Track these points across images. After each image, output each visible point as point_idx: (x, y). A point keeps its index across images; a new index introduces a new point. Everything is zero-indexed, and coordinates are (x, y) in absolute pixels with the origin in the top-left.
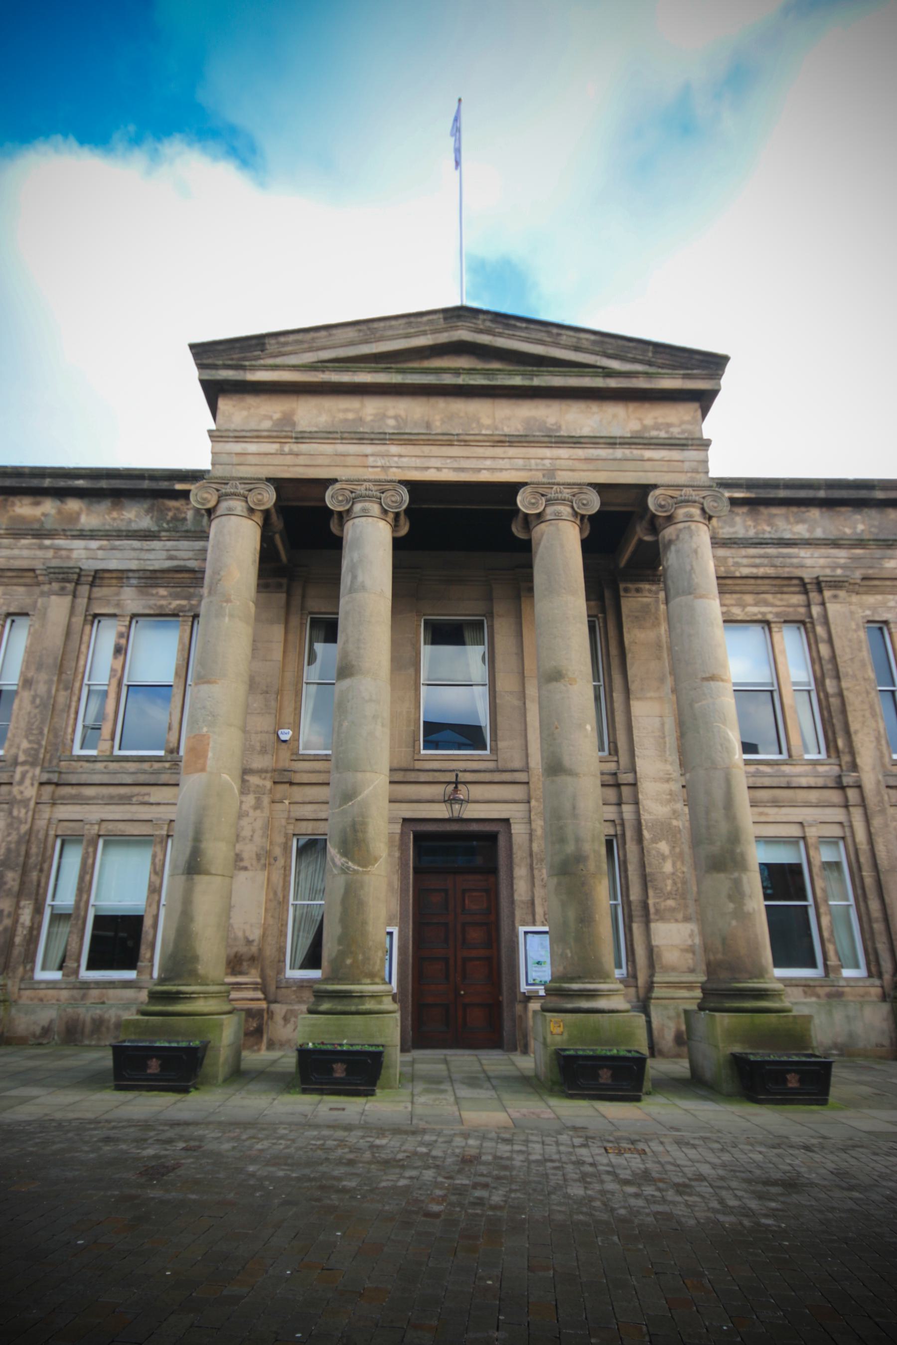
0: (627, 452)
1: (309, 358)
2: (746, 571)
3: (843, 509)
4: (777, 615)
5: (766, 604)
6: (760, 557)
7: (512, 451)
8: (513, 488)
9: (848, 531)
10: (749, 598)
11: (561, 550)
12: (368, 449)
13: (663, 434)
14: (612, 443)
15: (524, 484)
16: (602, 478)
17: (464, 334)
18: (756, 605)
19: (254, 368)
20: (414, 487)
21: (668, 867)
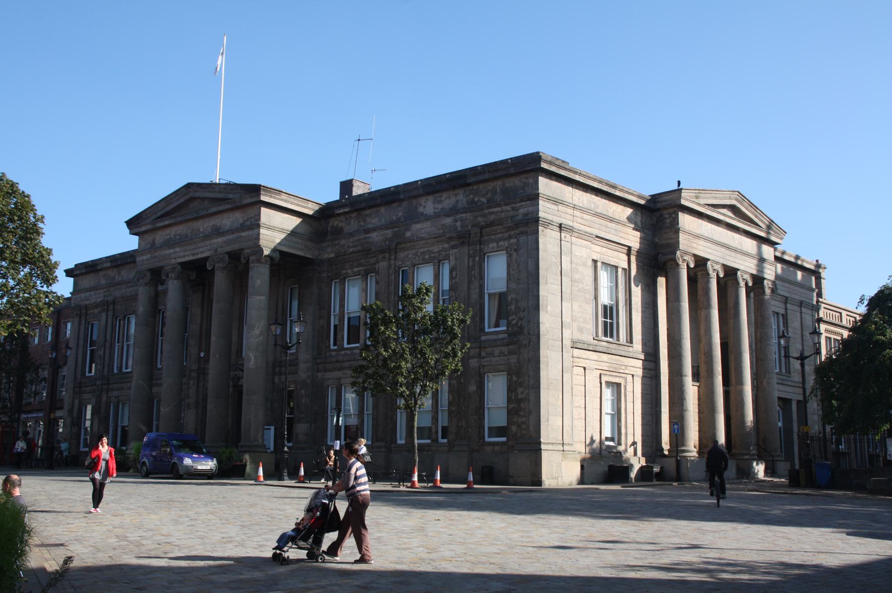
0: (236, 235)
1: (154, 217)
2: (351, 250)
3: (394, 205)
4: (365, 270)
5: (361, 265)
6: (358, 240)
7: (207, 243)
8: (206, 259)
9: (394, 218)
10: (355, 264)
11: (220, 281)
12: (172, 251)
13: (249, 223)
14: (231, 231)
15: (208, 257)
16: (229, 249)
17: (192, 194)
18: (357, 267)
19: (141, 227)
20: (180, 263)
21: (303, 401)
